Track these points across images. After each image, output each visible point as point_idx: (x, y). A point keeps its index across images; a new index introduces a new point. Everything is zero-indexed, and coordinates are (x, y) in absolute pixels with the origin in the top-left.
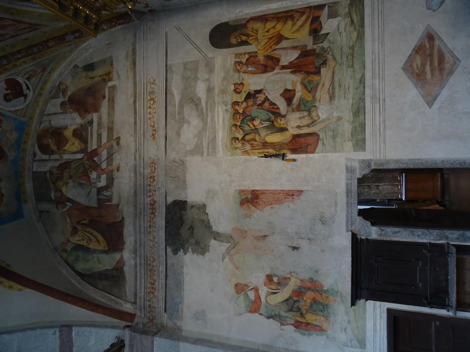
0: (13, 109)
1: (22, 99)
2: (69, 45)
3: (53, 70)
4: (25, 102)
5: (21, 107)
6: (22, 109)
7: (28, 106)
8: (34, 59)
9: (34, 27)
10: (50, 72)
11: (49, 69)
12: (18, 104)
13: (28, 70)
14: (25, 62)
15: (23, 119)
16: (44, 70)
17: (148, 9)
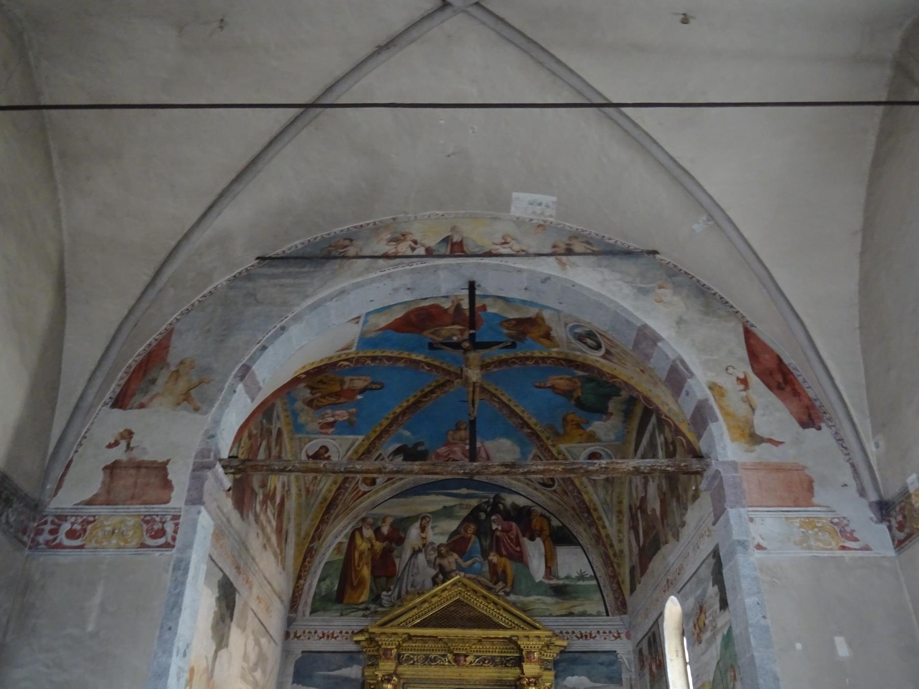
0: (314, 441)
1: (311, 454)
2: (307, 534)
3: (299, 495)
4: (306, 452)
5: (307, 446)
6: (305, 444)
7: (301, 450)
8: (325, 499)
9: (337, 516)
10: (300, 490)
11: (304, 493)
12: (312, 447)
13: (322, 484)
14: (329, 491)
15: (300, 436)
16: (308, 491)
17: (292, 635)
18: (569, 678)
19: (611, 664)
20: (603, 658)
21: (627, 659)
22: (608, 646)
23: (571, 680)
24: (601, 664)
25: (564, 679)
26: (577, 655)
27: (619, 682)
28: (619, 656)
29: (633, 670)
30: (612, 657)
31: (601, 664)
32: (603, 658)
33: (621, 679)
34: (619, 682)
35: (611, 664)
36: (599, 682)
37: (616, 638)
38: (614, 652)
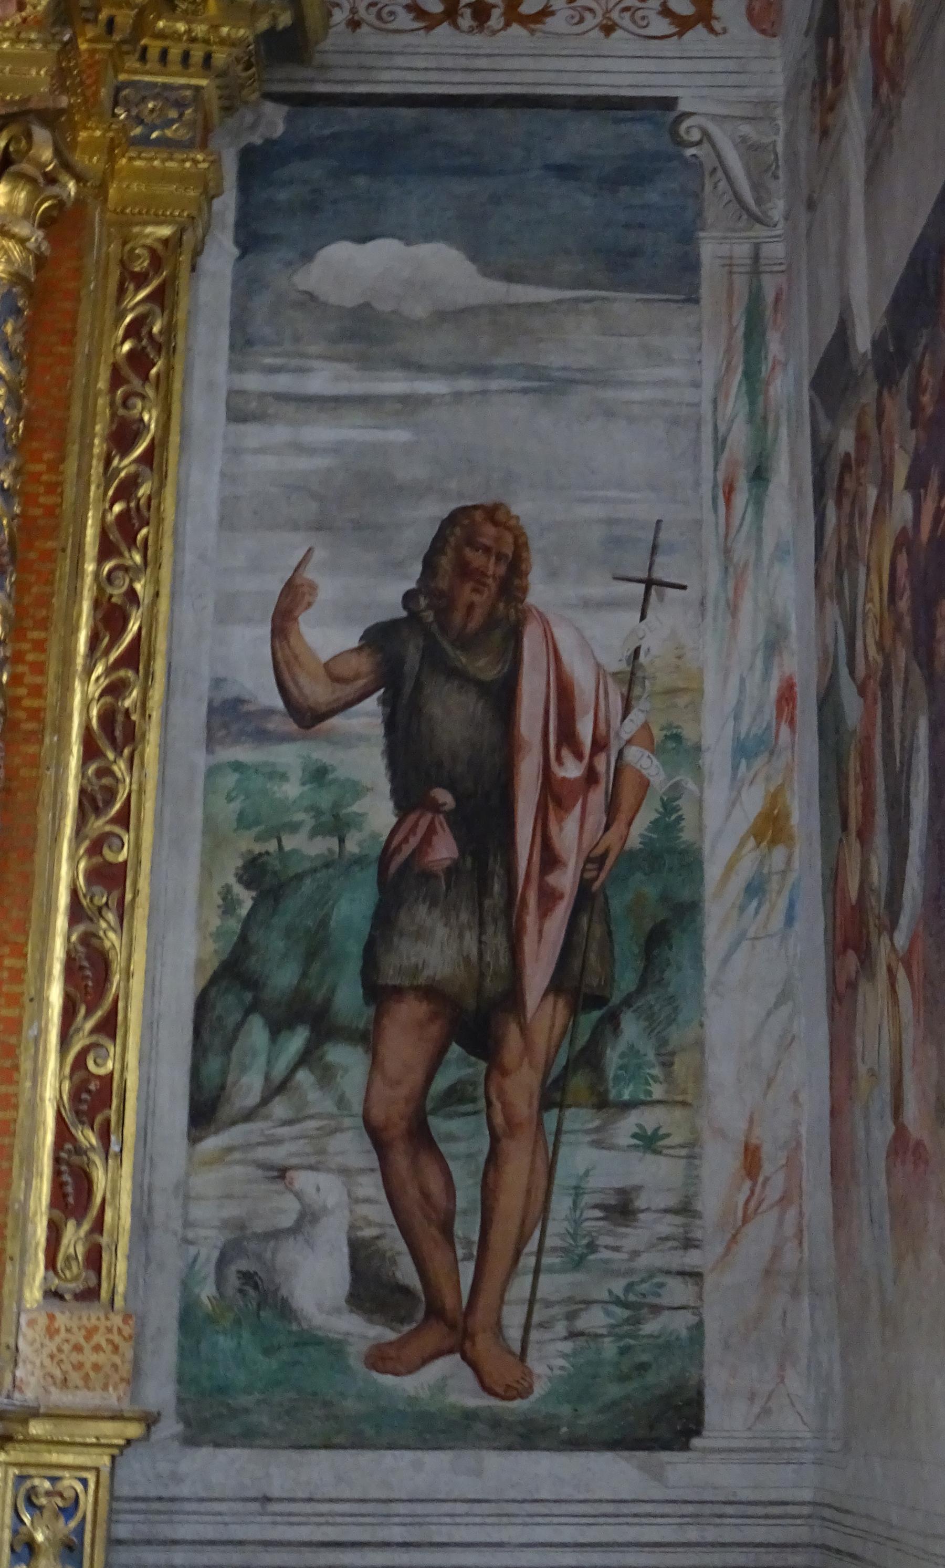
18: (340, 252)
19: (633, 172)
20: (580, 137)
21: (750, 149)
22: (622, 68)
23: (350, 267)
24: (565, 171)
25: (307, 256)
26: (407, 114)
27: (679, 278)
28: (690, 130)
29: (777, 209)
30: (642, 135)
31: (565, 171)
32: (580, 137)
33: (689, 266)
34: (679, 278)
35: (633, 172)
36: (547, 282)
37: (683, 24)
38: (668, 103)
